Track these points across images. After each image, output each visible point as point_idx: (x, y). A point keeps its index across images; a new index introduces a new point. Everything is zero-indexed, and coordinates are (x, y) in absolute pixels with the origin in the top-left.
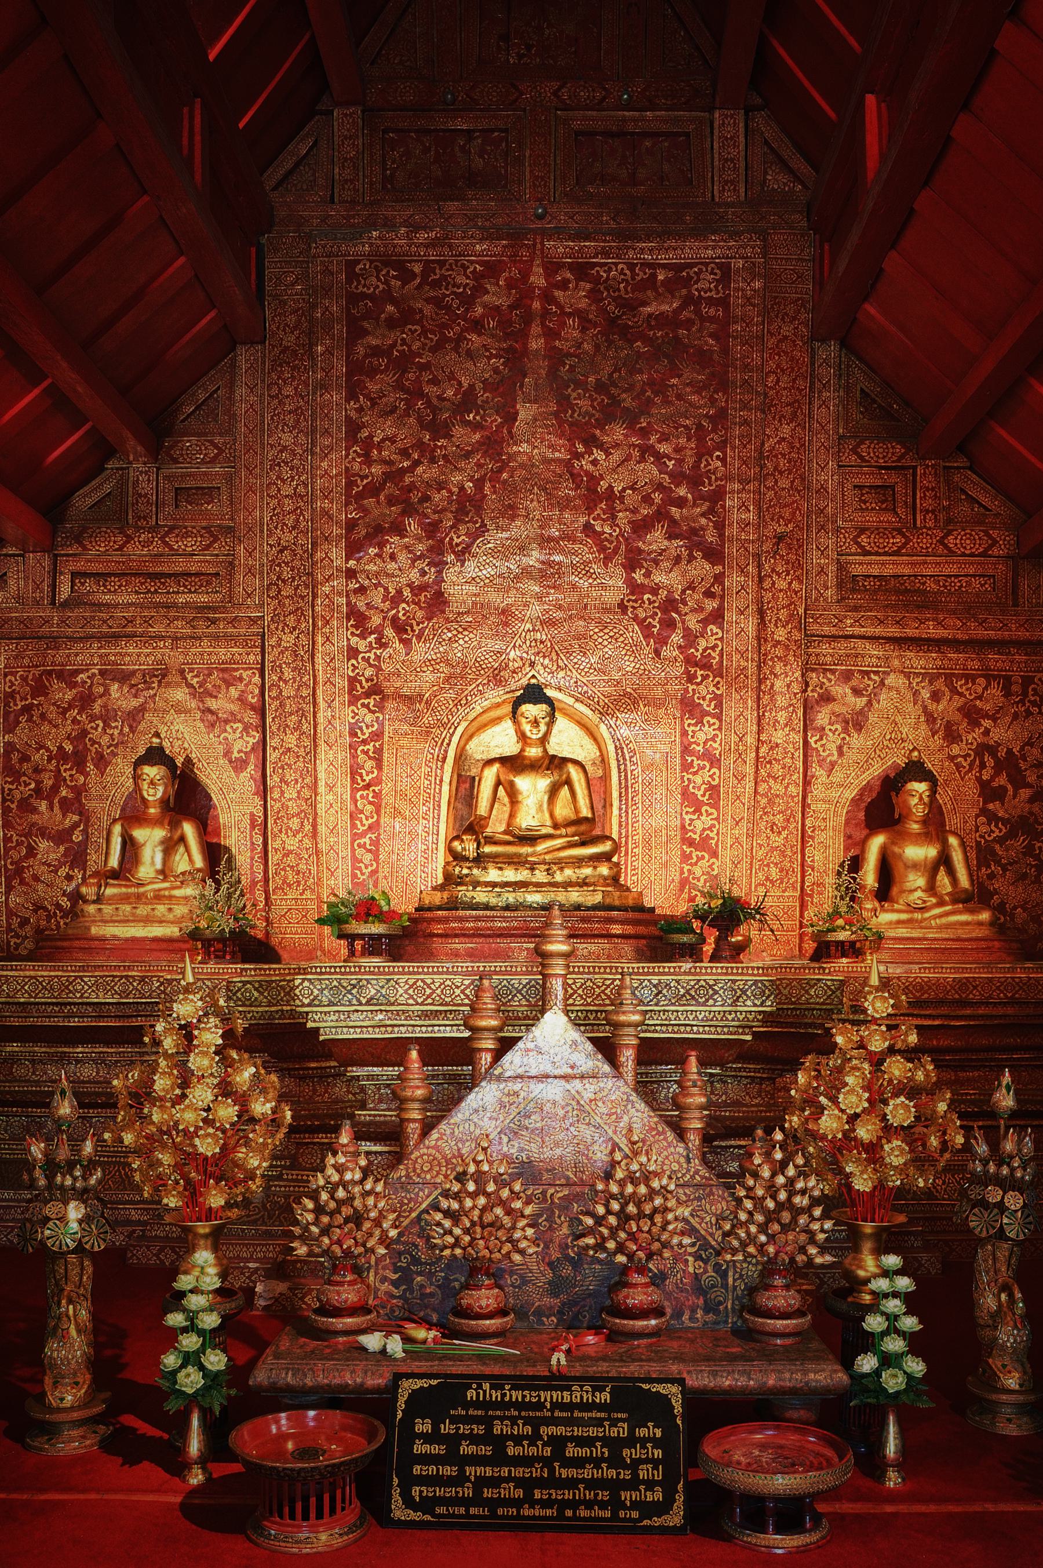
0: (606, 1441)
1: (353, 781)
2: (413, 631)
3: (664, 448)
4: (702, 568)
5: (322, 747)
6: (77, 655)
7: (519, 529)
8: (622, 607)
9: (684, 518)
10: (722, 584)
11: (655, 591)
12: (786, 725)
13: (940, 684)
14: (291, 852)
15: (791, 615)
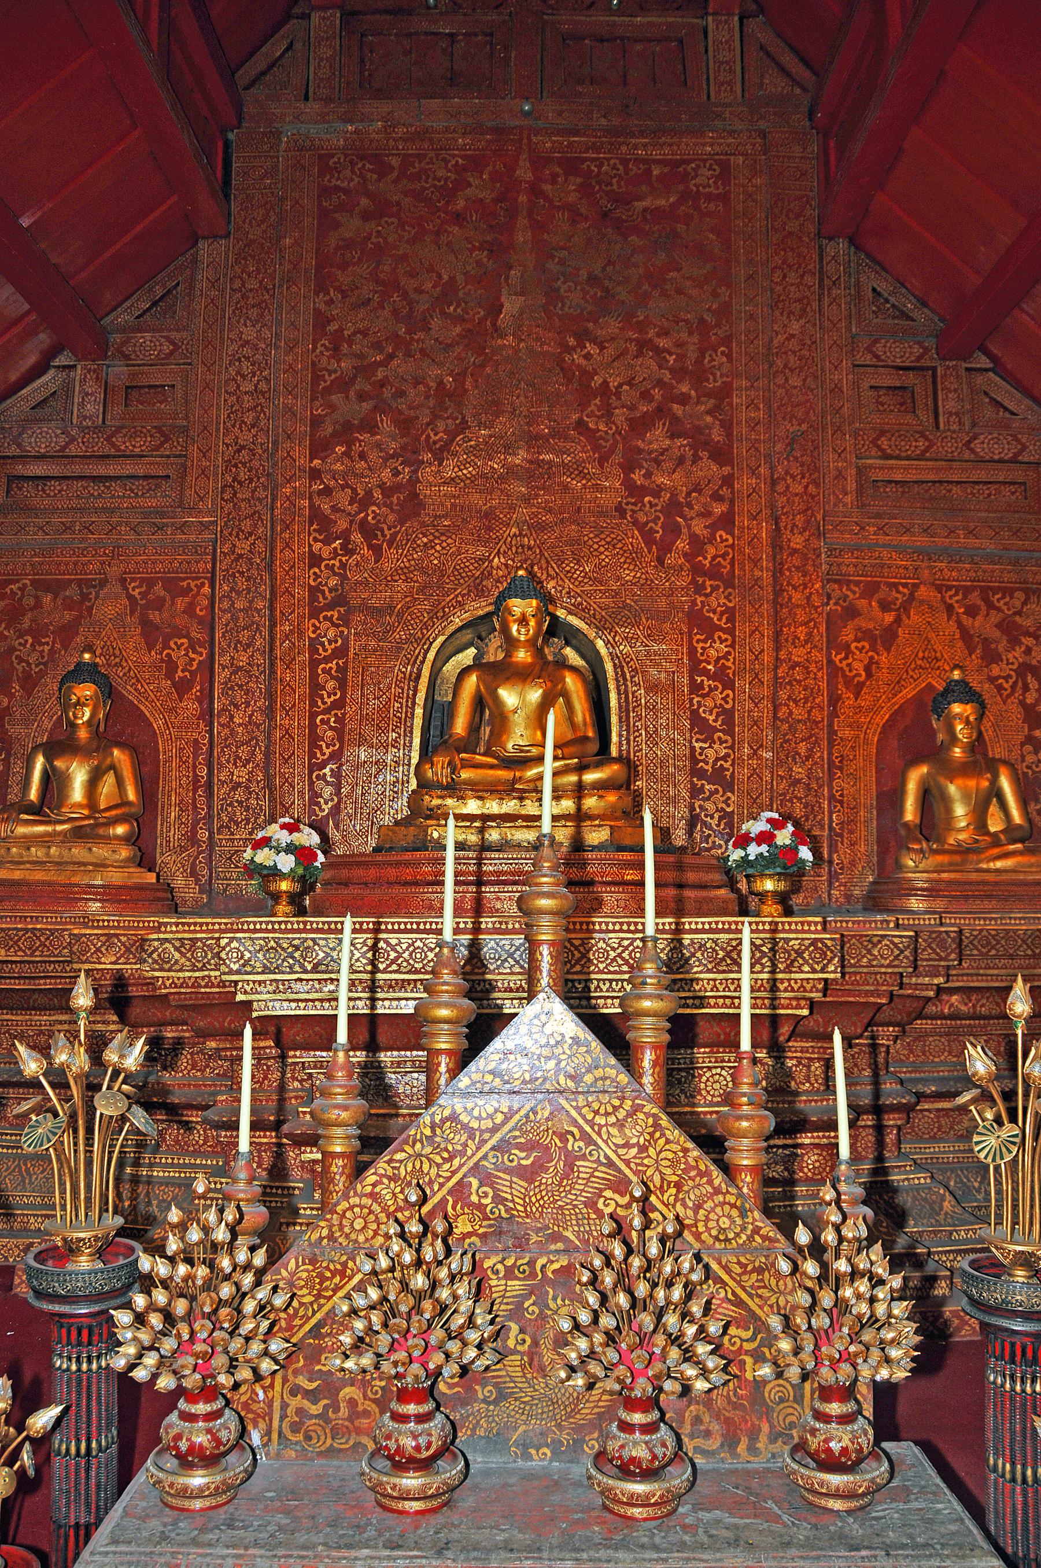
1: (313, 704)
2: (384, 536)
3: (662, 343)
4: (709, 469)
7: (506, 426)
8: (620, 511)
10: (731, 486)
11: (657, 493)
12: (806, 642)
13: (975, 598)
14: (239, 785)
15: (808, 522)
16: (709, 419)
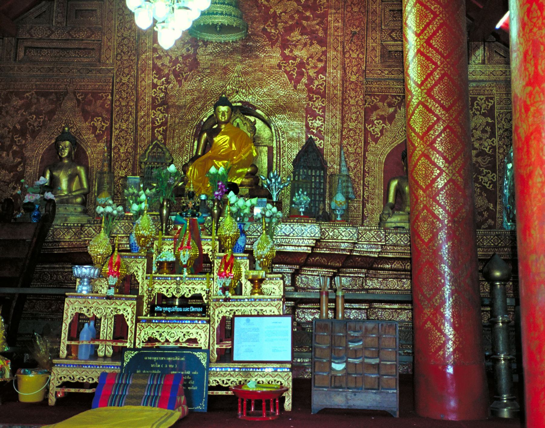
2: (183, 76)
4: (317, 48)
6: (25, 85)
8: (279, 66)
9: (309, 26)
12: (356, 120)
15: (359, 70)
16: (318, 27)
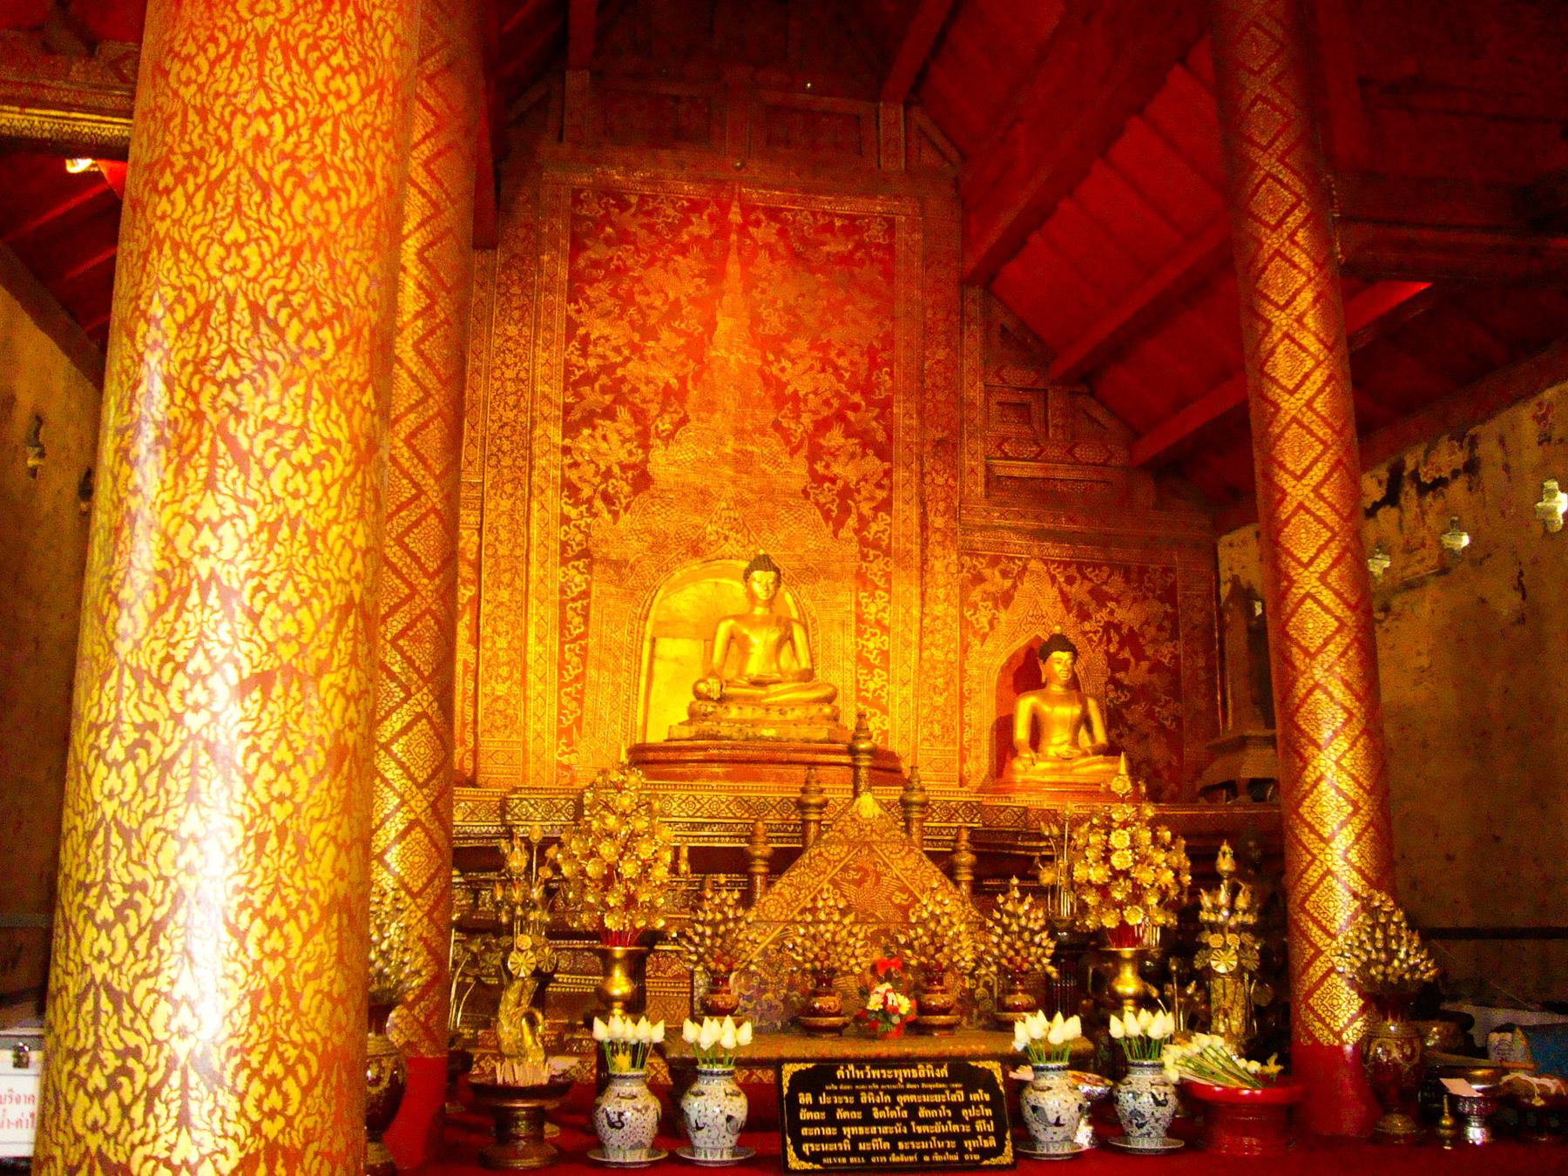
0: (949, 1105)
1: (562, 635)
4: (873, 464)
5: (533, 602)
8: (805, 493)
11: (833, 481)
13: (1072, 571)
15: (947, 508)
16: (874, 424)
